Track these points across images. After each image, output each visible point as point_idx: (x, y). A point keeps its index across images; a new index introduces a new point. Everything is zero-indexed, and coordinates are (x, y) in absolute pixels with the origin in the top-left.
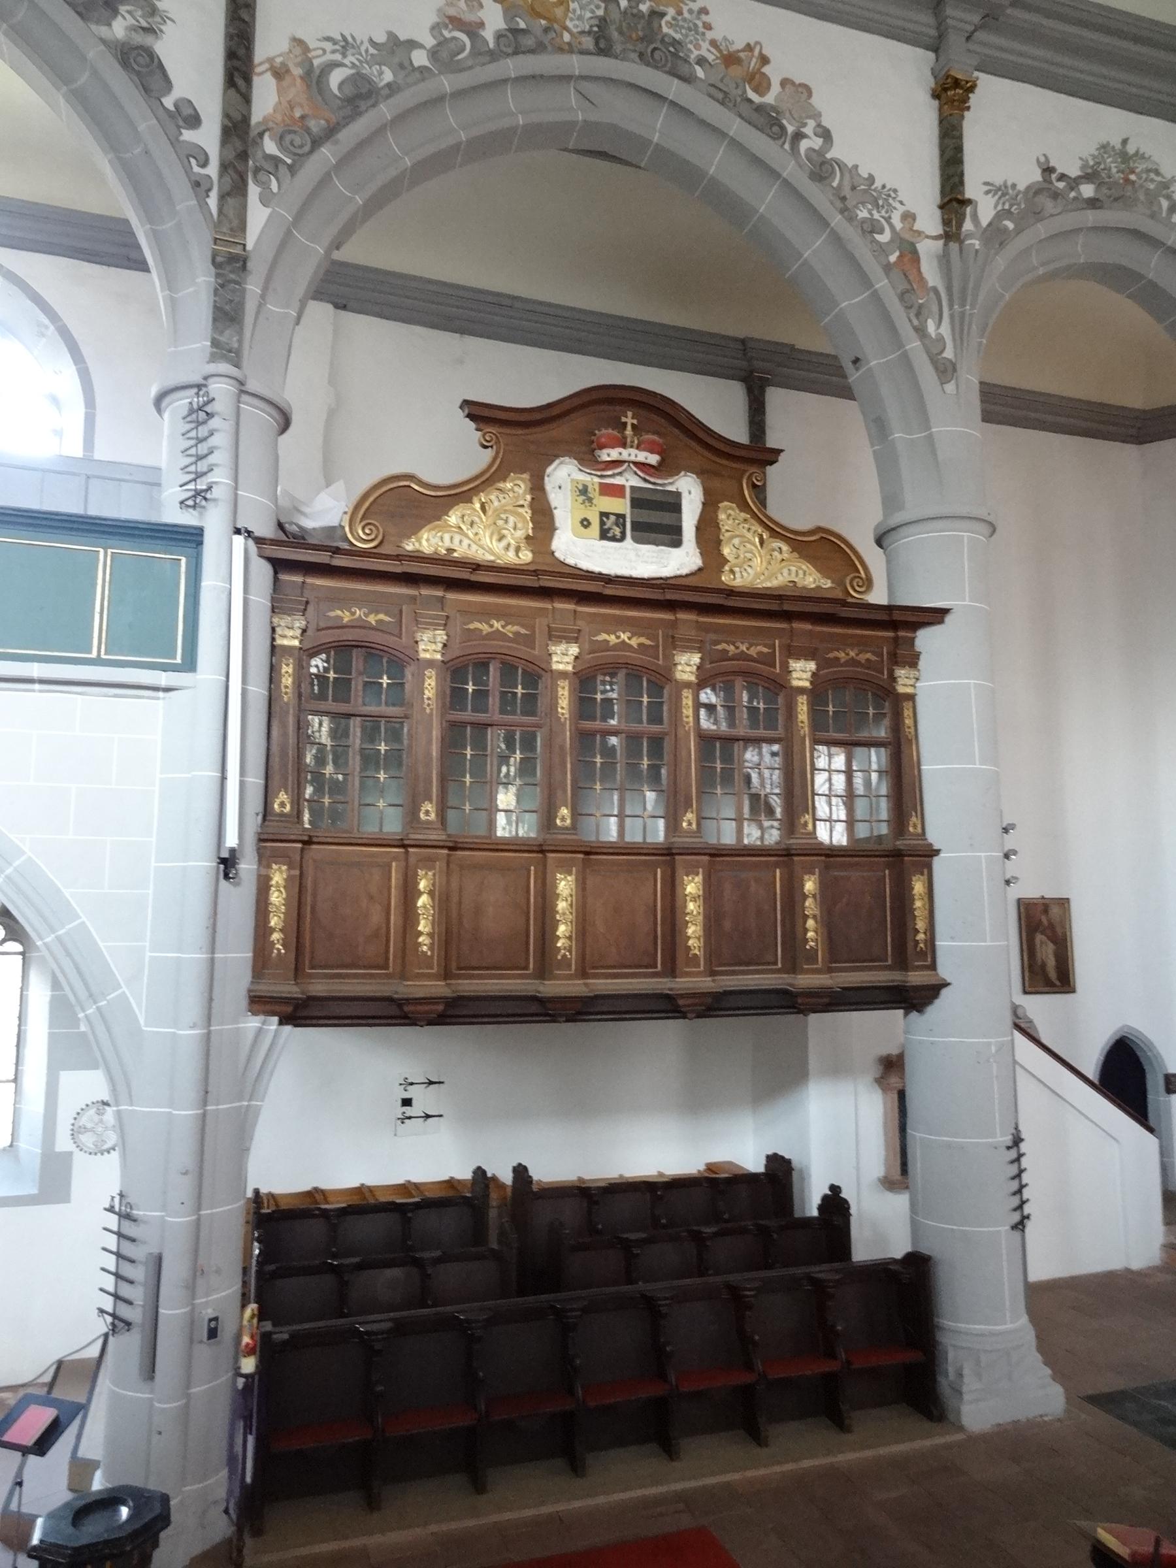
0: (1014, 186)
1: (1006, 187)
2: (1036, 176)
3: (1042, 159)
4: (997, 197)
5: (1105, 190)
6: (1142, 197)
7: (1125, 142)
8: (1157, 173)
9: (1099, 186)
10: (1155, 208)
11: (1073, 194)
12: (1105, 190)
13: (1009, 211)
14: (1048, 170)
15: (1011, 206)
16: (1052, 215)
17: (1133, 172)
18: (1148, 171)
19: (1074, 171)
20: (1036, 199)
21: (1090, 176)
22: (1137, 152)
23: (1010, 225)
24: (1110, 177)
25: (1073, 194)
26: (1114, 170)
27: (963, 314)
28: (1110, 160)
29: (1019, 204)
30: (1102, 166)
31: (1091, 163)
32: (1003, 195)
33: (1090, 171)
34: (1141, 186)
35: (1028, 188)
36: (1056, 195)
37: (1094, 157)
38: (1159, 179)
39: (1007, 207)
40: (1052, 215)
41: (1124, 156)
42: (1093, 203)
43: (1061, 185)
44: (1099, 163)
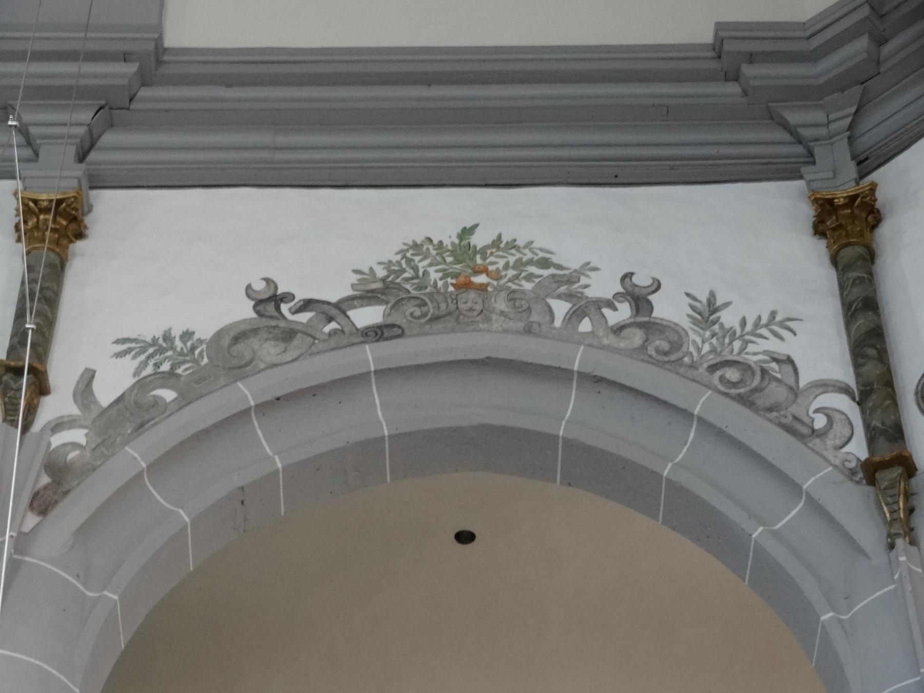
0: (187, 335)
2: (245, 311)
3: (259, 286)
4: (142, 357)
5: (411, 308)
6: (501, 304)
10: (535, 317)
12: (411, 308)
14: (270, 301)
18: (520, 264)
20: (240, 347)
22: (497, 242)
31: (381, 273)
32: (161, 350)
34: (499, 289)
37: (388, 265)
39: (166, 367)
42: (378, 333)
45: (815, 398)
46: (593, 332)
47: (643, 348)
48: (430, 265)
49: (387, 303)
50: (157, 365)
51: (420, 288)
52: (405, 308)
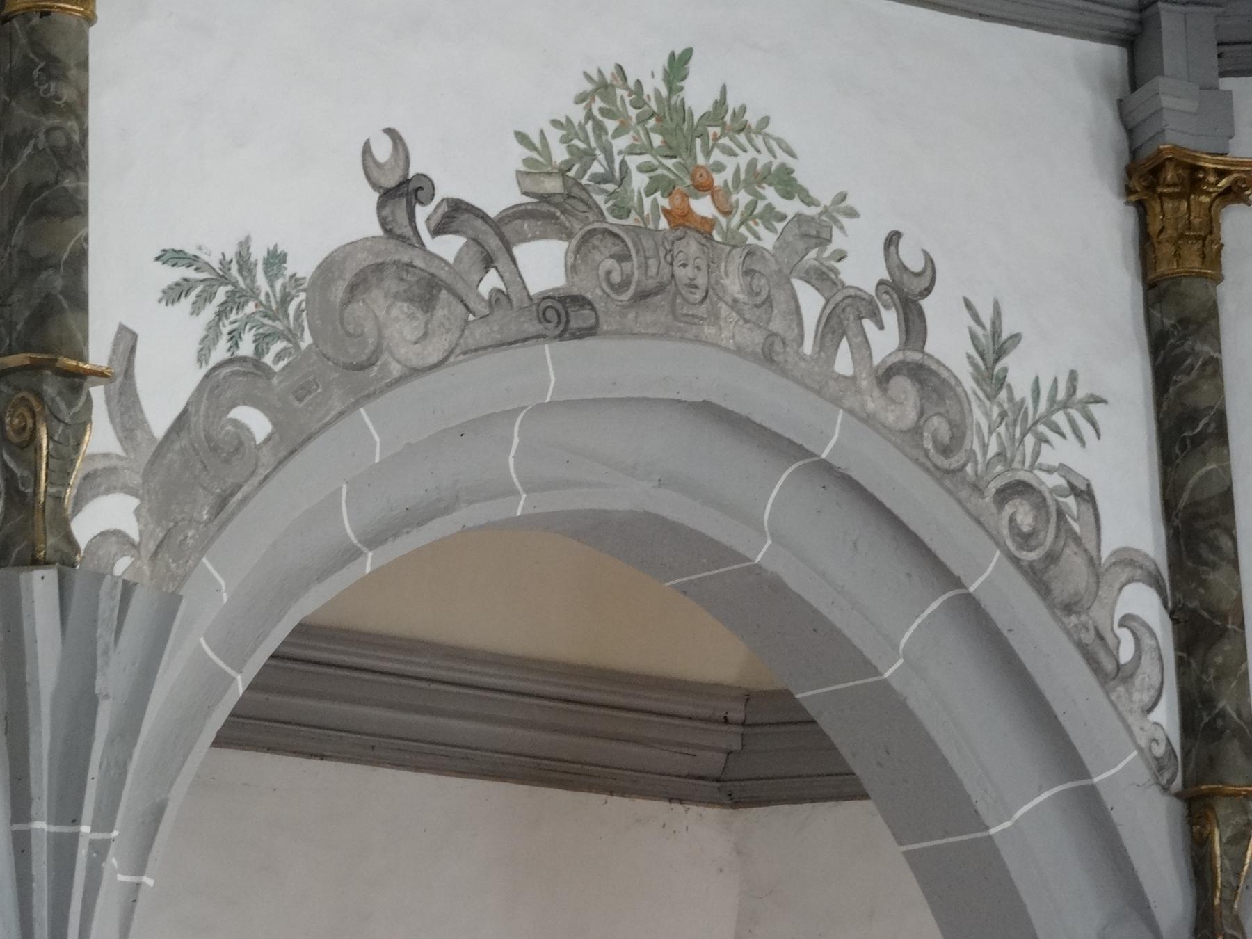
0: (276, 260)
1: (244, 261)
2: (360, 218)
3: (383, 150)
4: (210, 311)
6: (734, 285)
7: (677, 66)
8: (787, 184)
9: (583, 247)
10: (777, 325)
11: (491, 281)
13: (256, 365)
14: (402, 193)
15: (262, 341)
16: (414, 372)
17: (704, 187)
18: (755, 178)
19: (496, 194)
20: (357, 308)
21: (547, 211)
22: (721, 104)
23: (257, 423)
24: (621, 211)
25: (491, 281)
26: (639, 181)
27: (64, 849)
28: (621, 143)
29: (292, 336)
30: (597, 168)
31: (560, 154)
32: (236, 299)
33: (553, 185)
35: (328, 268)
36: (428, 289)
38: (791, 207)
39: (246, 348)
40: (414, 372)
41: (677, 128)
42: (563, 315)
43: (448, 247)
44: (587, 156)
45: (1121, 588)
46: (853, 379)
47: (916, 431)
48: (632, 151)
49: (569, 236)
50: (235, 337)
51: (621, 211)
52: (597, 256)
